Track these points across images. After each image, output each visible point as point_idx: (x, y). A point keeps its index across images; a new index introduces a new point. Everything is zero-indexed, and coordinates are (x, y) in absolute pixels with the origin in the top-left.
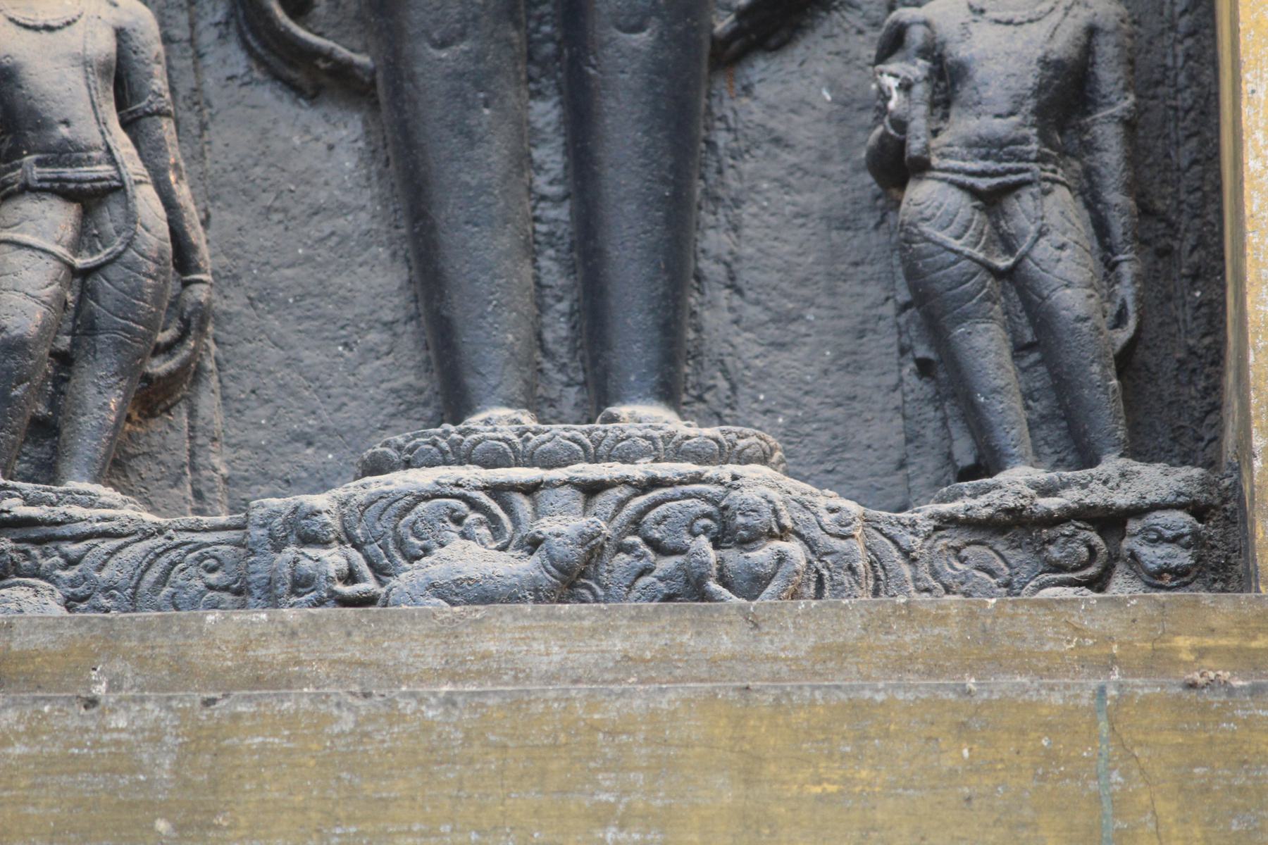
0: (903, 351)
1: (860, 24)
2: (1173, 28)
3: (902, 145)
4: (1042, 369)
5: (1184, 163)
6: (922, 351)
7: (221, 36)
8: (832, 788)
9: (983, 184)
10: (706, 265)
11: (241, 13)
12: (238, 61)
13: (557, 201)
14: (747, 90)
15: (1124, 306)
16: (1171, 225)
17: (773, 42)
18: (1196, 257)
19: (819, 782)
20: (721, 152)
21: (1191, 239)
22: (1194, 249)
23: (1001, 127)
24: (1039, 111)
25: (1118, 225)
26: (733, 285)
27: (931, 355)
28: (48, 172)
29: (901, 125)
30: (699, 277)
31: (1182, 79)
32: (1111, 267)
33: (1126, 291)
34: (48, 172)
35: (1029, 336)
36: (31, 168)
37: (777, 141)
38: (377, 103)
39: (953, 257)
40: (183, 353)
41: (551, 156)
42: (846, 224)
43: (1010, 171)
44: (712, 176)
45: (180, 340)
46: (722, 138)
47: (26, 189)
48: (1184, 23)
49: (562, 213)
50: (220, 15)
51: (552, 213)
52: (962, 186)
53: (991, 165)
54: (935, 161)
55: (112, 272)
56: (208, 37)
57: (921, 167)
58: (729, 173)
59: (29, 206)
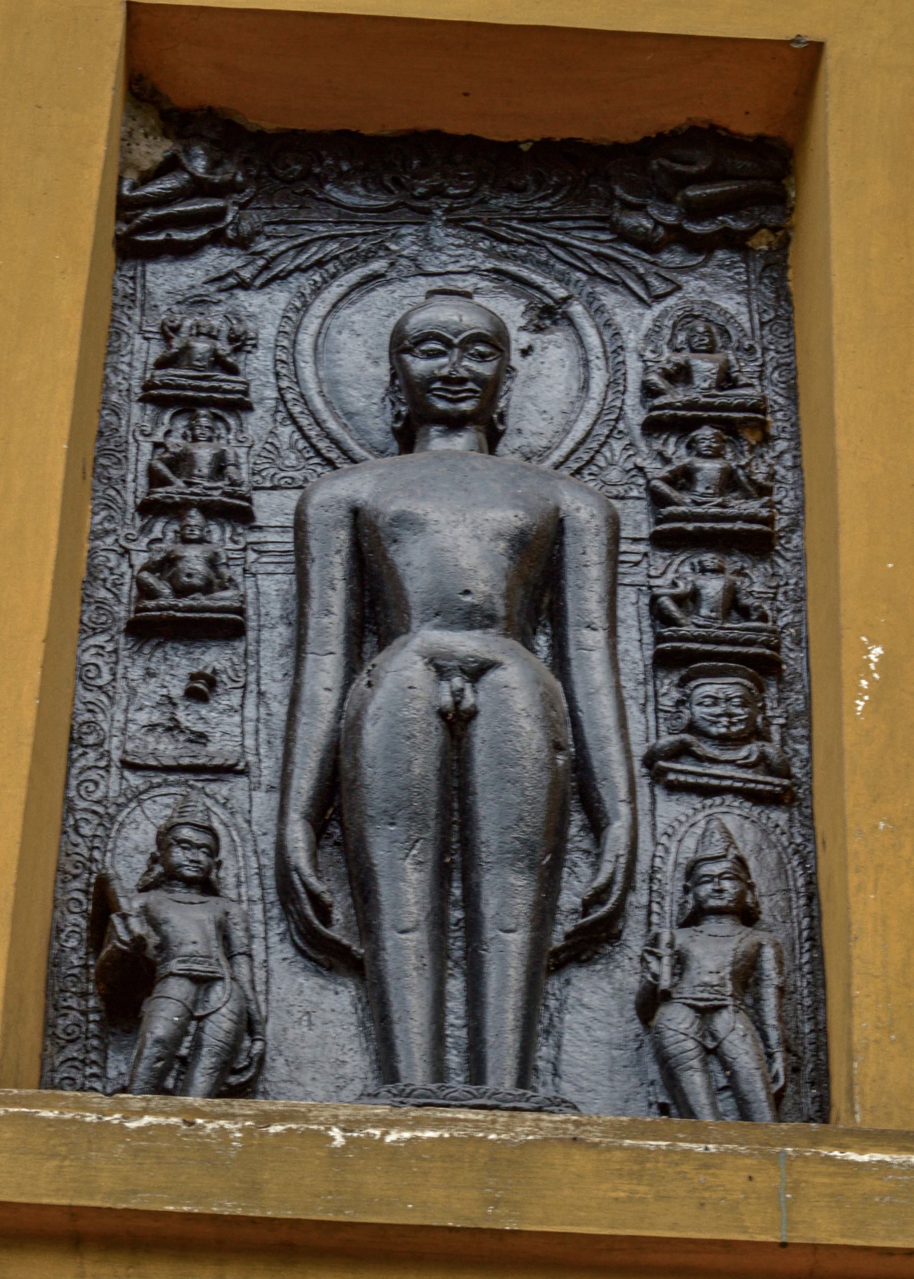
0: (650, 1105)
1: (631, 955)
2: (800, 969)
3: (656, 986)
4: (732, 1100)
5: (807, 1030)
6: (662, 1099)
7: (281, 941)
8: (622, 1194)
9: (701, 1004)
10: (541, 1064)
11: (293, 926)
12: (288, 951)
13: (459, 1028)
14: (568, 982)
15: (777, 1073)
16: (799, 1058)
17: (584, 957)
18: (813, 1074)
19: (615, 1189)
20: (552, 1010)
21: (811, 1066)
22: (812, 1070)
23: (714, 979)
24: (734, 974)
25: (774, 1036)
26: (556, 1074)
27: (667, 1101)
28: (183, 966)
29: (656, 977)
30: (536, 1069)
31: (806, 992)
32: (770, 1056)
33: (779, 1065)
34: (183, 966)
35: (723, 1082)
36: (175, 966)
37: (583, 1005)
38: (364, 975)
39: (682, 1037)
40: (249, 1075)
41: (456, 1006)
42: (619, 1047)
43: (716, 999)
44: (546, 1021)
45: (246, 1068)
46: (552, 1003)
47: (172, 974)
48: (806, 968)
49: (463, 1033)
50: (280, 930)
51: (457, 1033)
52: (689, 1006)
53: (706, 995)
54: (675, 995)
55: (212, 1018)
56: (274, 939)
57: (666, 997)
58: (556, 1019)
59: (172, 981)
